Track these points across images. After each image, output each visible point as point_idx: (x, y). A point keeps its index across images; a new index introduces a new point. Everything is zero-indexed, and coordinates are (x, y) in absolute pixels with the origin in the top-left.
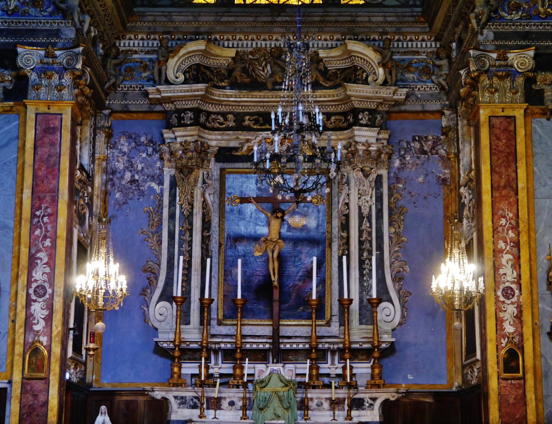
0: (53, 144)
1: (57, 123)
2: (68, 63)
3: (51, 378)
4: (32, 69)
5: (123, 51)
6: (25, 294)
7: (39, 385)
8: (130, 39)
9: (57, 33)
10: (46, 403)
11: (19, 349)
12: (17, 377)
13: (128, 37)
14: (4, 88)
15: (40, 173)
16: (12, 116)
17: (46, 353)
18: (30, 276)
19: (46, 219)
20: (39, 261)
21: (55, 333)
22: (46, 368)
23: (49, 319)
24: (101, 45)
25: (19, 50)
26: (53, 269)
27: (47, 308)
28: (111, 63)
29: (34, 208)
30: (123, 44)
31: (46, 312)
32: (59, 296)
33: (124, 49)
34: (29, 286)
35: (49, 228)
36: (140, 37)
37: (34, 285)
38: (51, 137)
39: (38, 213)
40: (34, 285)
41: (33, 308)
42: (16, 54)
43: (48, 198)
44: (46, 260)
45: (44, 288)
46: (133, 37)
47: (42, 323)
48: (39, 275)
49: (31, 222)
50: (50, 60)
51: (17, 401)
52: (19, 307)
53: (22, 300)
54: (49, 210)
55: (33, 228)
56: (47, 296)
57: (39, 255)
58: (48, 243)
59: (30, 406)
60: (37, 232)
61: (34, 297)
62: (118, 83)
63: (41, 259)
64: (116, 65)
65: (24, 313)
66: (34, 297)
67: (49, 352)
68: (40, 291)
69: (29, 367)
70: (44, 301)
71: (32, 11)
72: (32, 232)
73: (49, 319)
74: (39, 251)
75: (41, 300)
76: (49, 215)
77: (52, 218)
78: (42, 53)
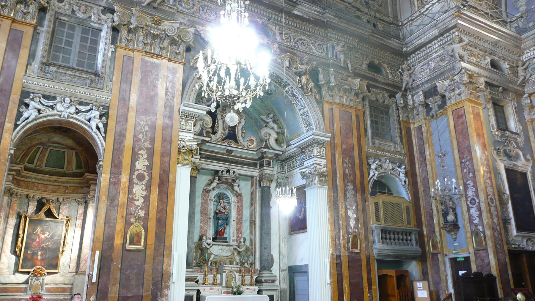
0: (463, 123)
1: (462, 112)
2: (460, 80)
3: (488, 249)
4: (446, 91)
5: (526, 61)
6: (466, 205)
7: (483, 253)
8: (528, 53)
9: (453, 69)
10: (489, 264)
11: (469, 235)
12: (472, 250)
13: (525, 52)
14: (438, 105)
15: (460, 140)
16: (444, 116)
17: (482, 235)
18: (466, 195)
19: (467, 163)
20: (469, 186)
21: (485, 223)
22: (484, 243)
23: (480, 216)
24: (506, 63)
25: (438, 84)
26: (477, 189)
27: (478, 210)
28: (520, 69)
29: (461, 158)
30: (524, 57)
31: (478, 213)
32: (482, 202)
33: (526, 59)
34: (467, 200)
35: (470, 166)
36: (532, 49)
37: (469, 199)
38: (461, 120)
39: (463, 161)
40: (469, 199)
41: (471, 211)
42: (437, 87)
43: (466, 152)
44: (472, 184)
45: (474, 199)
46: (528, 51)
47: (477, 219)
48: (470, 193)
49: (461, 166)
50: (452, 83)
51: (474, 263)
52: (465, 212)
53: (465, 208)
54: (468, 158)
55: (462, 169)
56: (477, 204)
57: (468, 182)
58: (471, 175)
59: (481, 266)
60: (465, 171)
61: (470, 206)
62: (527, 78)
63: (469, 184)
64: (525, 69)
65: (467, 215)
66: (470, 206)
67: (484, 234)
68: (473, 202)
69: (476, 244)
70: (476, 207)
71: (441, 64)
72: (462, 171)
73: (480, 216)
74: (468, 180)
75: (474, 206)
76: (469, 160)
77: (470, 161)
78: (448, 81)
